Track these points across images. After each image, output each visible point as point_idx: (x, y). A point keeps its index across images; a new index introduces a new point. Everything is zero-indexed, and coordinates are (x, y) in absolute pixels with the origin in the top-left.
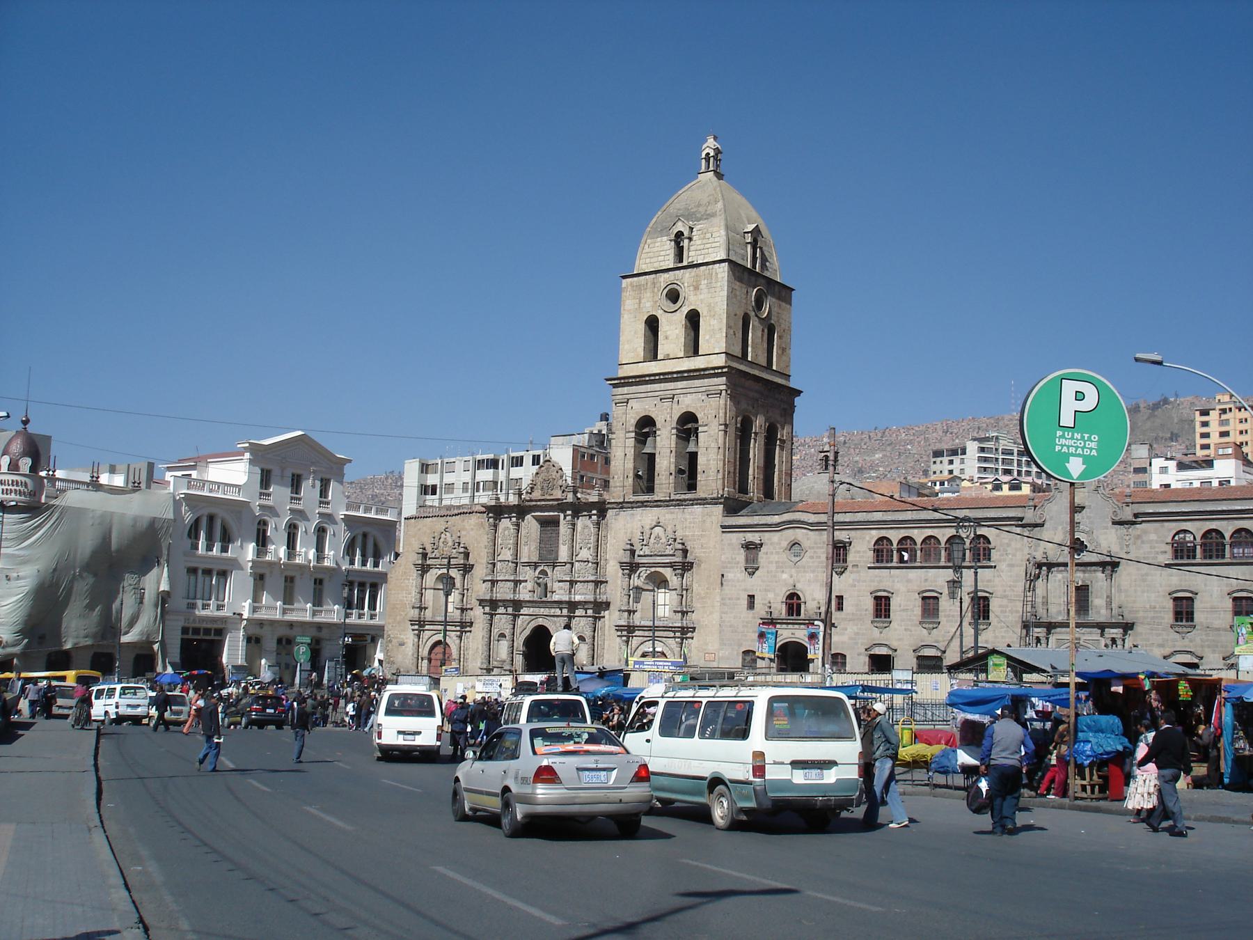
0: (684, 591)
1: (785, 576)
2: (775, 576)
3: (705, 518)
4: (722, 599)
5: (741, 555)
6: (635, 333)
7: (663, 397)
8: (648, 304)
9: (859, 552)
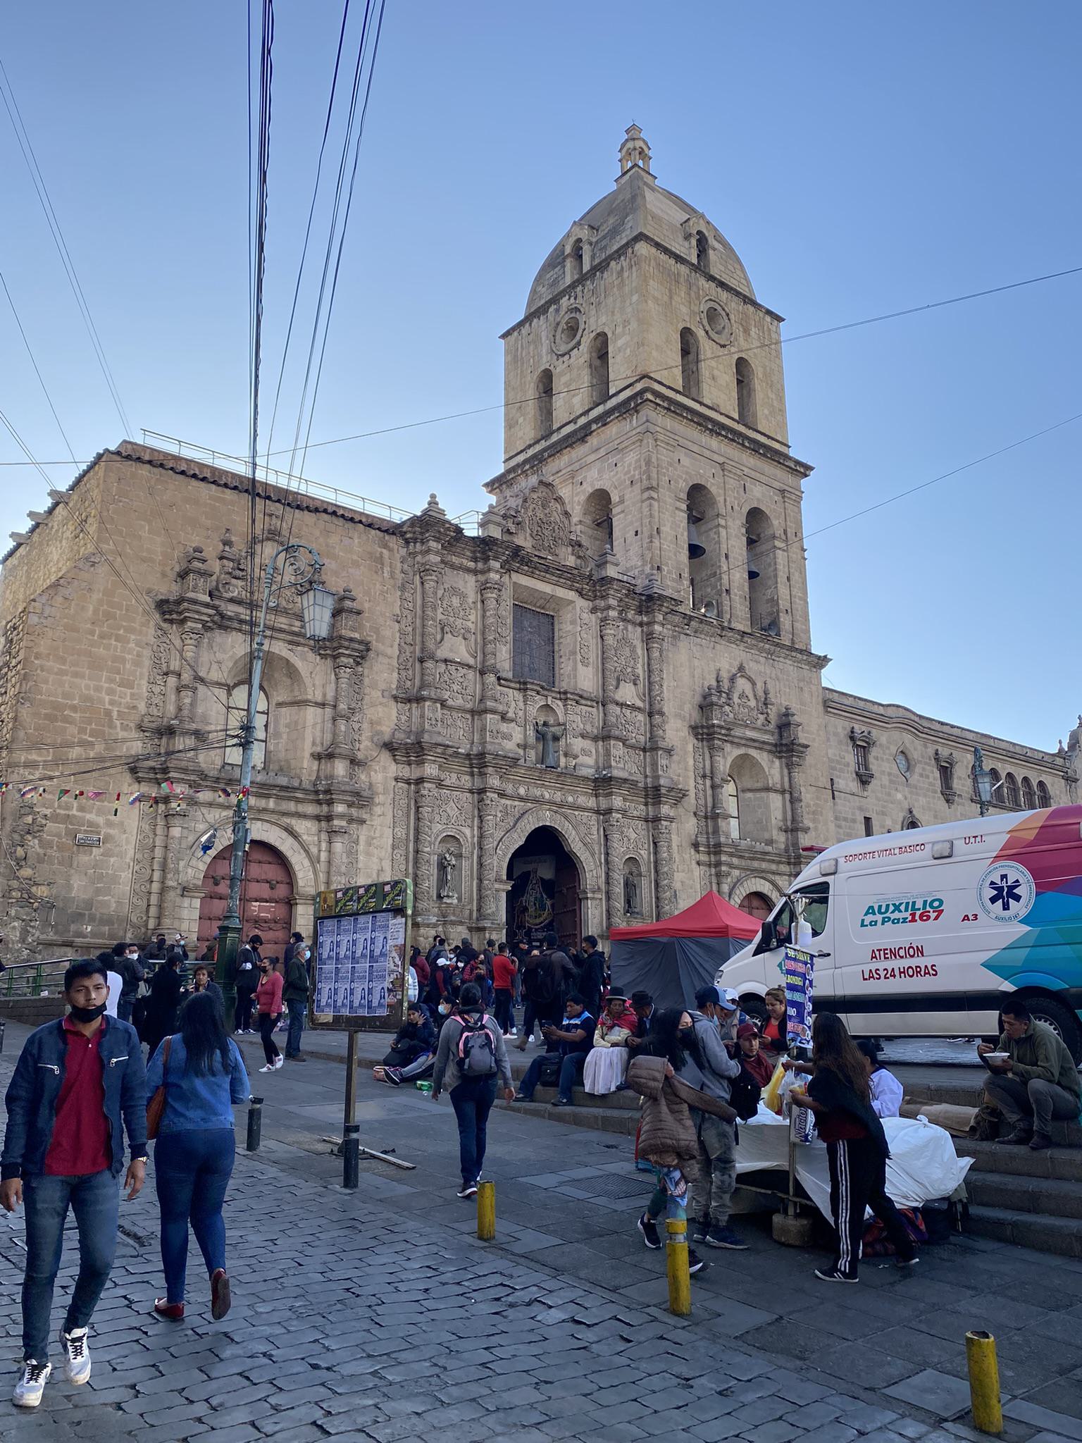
0: (792, 796)
1: (899, 796)
2: (889, 794)
3: (801, 684)
4: (837, 818)
5: (850, 757)
6: (668, 341)
7: (730, 468)
8: (684, 310)
9: (960, 778)
